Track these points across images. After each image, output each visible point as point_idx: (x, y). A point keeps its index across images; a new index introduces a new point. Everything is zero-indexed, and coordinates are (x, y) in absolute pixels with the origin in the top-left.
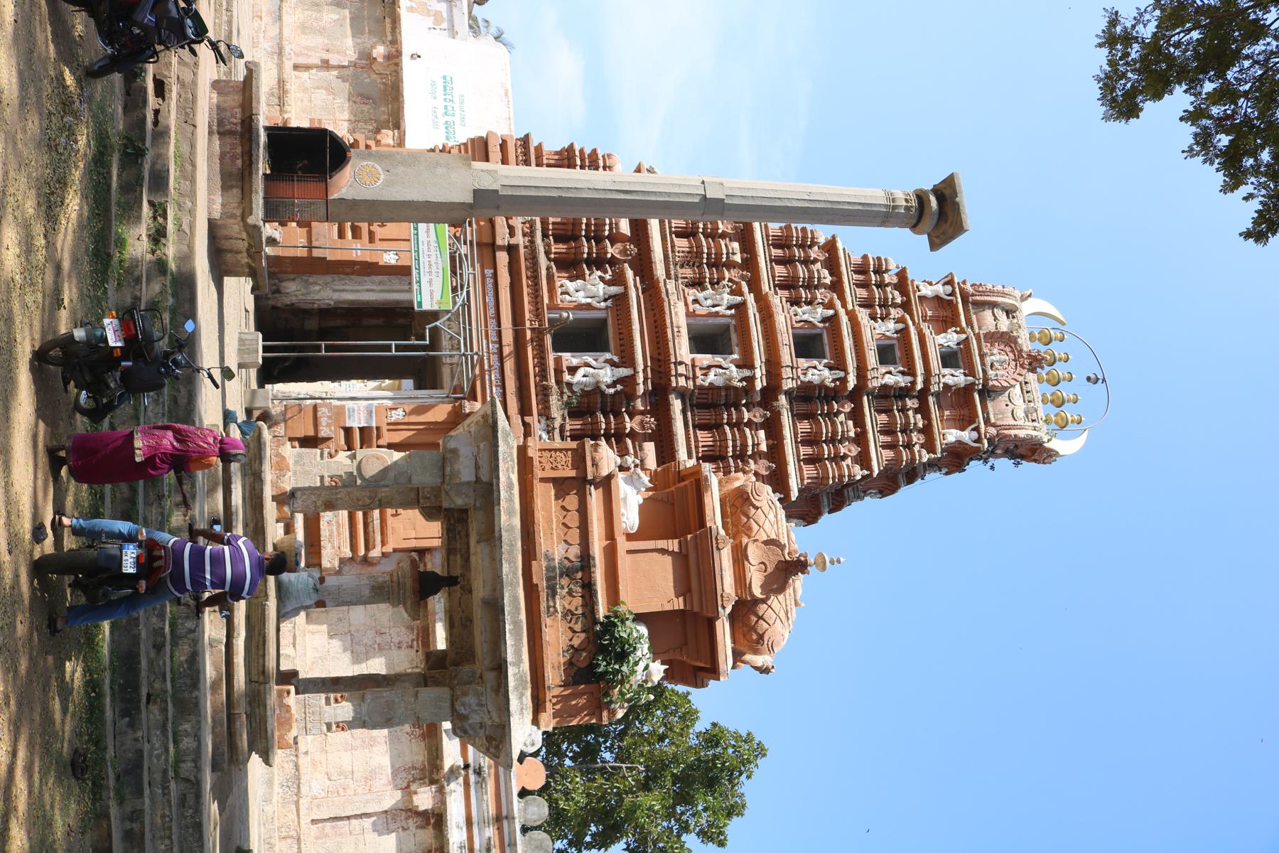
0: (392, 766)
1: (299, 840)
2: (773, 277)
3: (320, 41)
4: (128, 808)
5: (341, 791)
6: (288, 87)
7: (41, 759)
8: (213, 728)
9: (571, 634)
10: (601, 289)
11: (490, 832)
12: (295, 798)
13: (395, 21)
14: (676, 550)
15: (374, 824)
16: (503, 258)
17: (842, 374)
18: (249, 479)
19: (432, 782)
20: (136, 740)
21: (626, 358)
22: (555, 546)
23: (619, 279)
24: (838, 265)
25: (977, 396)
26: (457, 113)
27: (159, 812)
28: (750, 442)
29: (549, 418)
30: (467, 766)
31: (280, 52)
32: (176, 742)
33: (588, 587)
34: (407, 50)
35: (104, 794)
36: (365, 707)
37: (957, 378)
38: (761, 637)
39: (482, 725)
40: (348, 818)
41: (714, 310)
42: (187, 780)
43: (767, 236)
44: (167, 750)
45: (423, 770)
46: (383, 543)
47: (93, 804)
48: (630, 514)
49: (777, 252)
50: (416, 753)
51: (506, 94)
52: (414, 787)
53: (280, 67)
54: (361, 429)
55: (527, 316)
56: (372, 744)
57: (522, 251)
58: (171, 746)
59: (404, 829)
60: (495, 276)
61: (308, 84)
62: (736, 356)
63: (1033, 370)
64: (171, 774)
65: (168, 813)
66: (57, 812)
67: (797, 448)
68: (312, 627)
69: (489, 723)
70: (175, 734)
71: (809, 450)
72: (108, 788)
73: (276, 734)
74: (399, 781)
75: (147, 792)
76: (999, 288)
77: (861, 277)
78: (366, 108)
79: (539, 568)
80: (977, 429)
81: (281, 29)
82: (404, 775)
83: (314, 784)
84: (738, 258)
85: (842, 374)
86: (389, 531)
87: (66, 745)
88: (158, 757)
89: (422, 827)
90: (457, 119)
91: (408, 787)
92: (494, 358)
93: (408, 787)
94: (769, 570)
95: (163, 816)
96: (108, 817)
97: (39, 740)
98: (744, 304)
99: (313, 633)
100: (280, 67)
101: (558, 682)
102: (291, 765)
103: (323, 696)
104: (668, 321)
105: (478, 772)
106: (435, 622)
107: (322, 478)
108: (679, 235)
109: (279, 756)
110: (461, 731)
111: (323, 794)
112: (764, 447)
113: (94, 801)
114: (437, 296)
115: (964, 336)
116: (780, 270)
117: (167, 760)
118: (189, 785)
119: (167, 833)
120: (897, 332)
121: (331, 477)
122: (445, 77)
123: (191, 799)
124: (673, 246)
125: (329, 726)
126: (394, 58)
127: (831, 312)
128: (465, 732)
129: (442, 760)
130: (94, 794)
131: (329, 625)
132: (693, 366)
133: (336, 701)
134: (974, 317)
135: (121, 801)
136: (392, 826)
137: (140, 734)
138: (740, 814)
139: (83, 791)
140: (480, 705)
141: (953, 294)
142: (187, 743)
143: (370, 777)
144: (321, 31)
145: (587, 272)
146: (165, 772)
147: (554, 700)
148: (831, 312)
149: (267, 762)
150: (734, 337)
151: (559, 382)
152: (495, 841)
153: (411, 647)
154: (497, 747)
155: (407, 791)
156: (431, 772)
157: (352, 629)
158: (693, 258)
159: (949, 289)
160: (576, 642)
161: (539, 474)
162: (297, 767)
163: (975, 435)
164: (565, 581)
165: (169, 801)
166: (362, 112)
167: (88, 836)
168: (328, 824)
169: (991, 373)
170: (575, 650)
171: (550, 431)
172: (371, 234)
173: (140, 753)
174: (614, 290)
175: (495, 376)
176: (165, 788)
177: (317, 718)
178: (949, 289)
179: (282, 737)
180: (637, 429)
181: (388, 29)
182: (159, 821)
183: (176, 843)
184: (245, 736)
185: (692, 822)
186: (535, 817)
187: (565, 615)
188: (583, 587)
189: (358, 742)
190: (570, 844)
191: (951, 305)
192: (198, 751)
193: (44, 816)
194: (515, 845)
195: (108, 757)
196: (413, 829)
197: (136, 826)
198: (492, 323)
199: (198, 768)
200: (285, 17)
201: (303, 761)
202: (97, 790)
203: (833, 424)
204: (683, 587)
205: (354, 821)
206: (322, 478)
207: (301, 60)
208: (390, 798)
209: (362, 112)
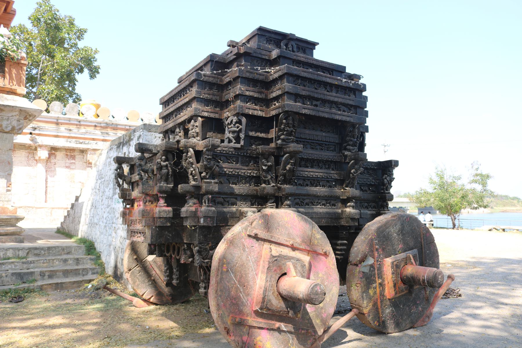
0: (26, 166)
1: (53, 208)
4: (39, 277)
7: (15, 316)
8: (2, 242)
11: (62, 128)
12: (34, 209)
15: (51, 176)
19: (36, 149)
20: (6, 276)
27: (42, 264)
30: (31, 133)
32: (9, 259)
35: (32, 288)
39: (18, 121)
40: (46, 187)
42: (28, 253)
44: (13, 263)
47: (36, 292)
52: (37, 158)
58: (10, 261)
59: (55, 164)
64: (24, 260)
65: (42, 261)
66: (40, 306)
69: (18, 117)
70: (5, 259)
72: (29, 287)
73: (9, 214)
74: (33, 164)
75: (32, 270)
82: (30, 162)
87: (7, 306)
88: (15, 266)
89: (55, 157)
91: (36, 160)
93: (36, 160)
95: (44, 263)
96: (42, 286)
97: (6, 318)
105: (35, 129)
109: (20, 213)
110: (19, 131)
113: (34, 292)
117: (18, 262)
118: (30, 252)
119: (51, 261)
123: (36, 252)
125: (8, 191)
128: (20, 129)
129: (26, 144)
130: (31, 292)
135: (36, 281)
136: (53, 169)
137: (4, 275)
138: (74, 20)
139: (30, 297)
140: (8, 119)
142: (10, 254)
146: (23, 263)
147: (11, 84)
149: (22, 219)
152: (67, 127)
154: (30, 116)
156: (31, 149)
165: (37, 261)
167: (49, 293)
168: (48, 196)
173: (13, 274)
176: (31, 262)
179: (11, 212)
182: (45, 265)
183: (56, 257)
184: (8, 228)
185: (73, 41)
186: (59, 108)
190: (71, 96)
192: (14, 249)
193: (42, 311)
194: (70, 119)
195: (14, 288)
196: (55, 161)
197: (47, 274)
199: (23, 249)
202: (29, 291)
205: (48, 185)
208: (40, 168)
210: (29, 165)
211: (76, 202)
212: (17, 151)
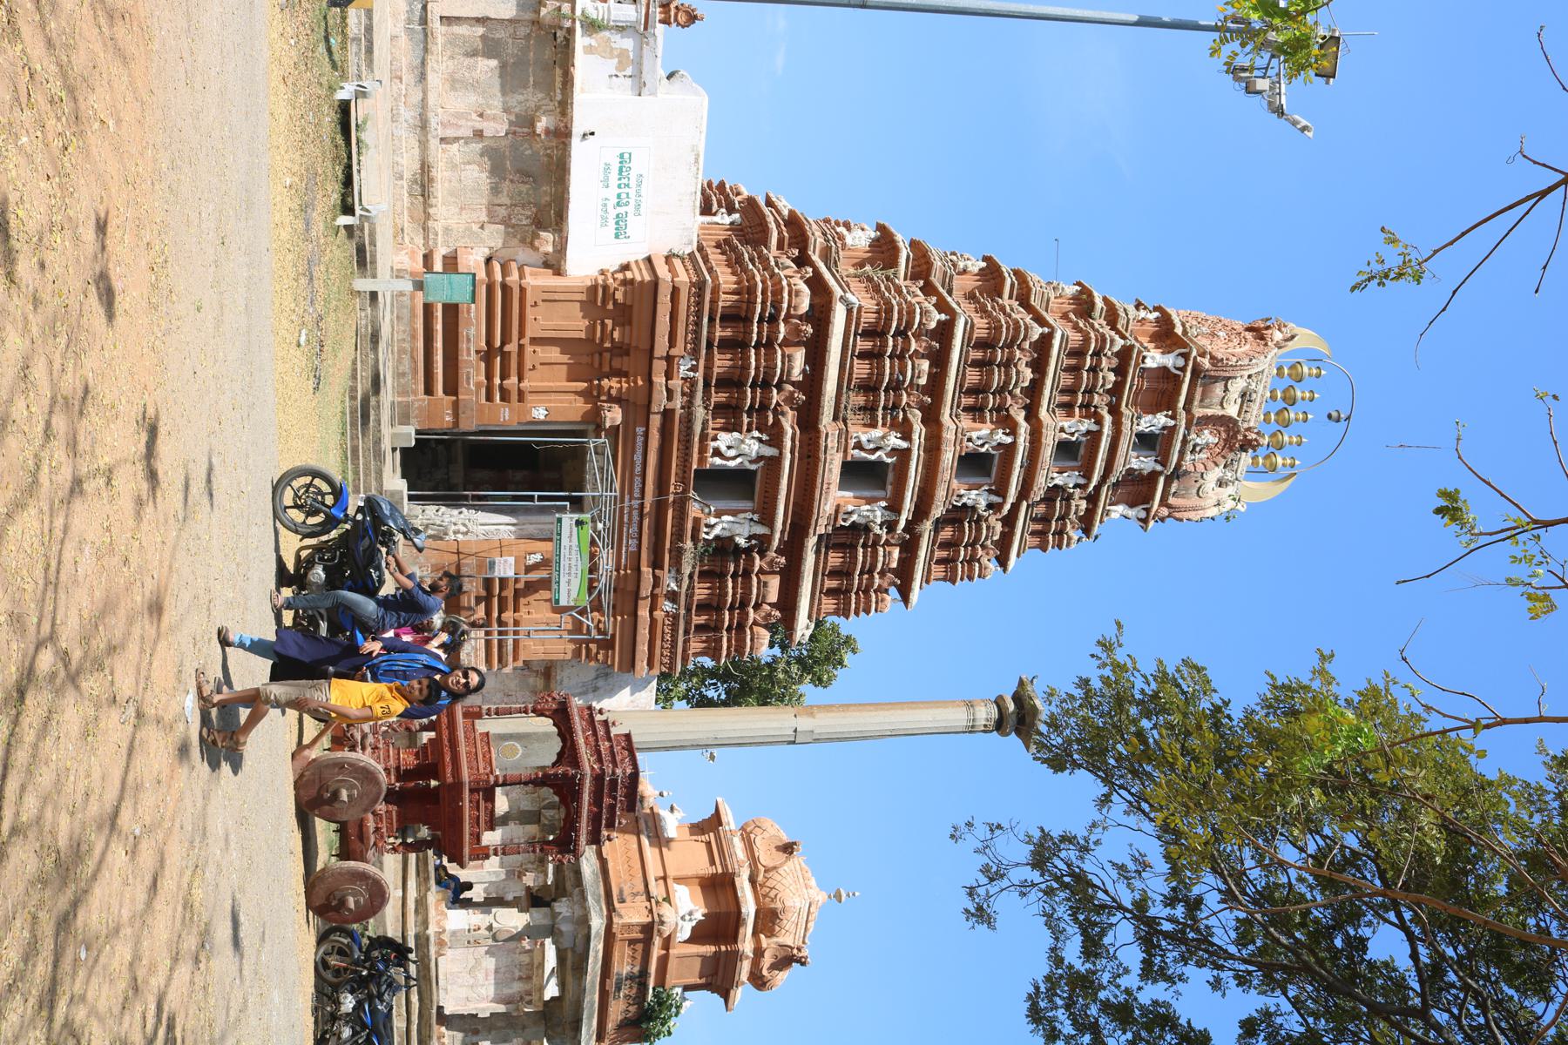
2: (961, 386)
3: (472, 98)
6: (434, 173)
10: (752, 446)
13: (568, 81)
16: (656, 421)
17: (999, 500)
21: (767, 518)
23: (775, 439)
24: (1046, 363)
25: (1162, 480)
26: (632, 202)
28: (879, 566)
29: (679, 571)
31: (424, 125)
33: (643, 986)
34: (577, 129)
37: (1144, 463)
38: (764, 984)
41: (873, 457)
43: (970, 339)
46: (515, 659)
49: (976, 355)
51: (697, 161)
53: (423, 145)
54: (501, 580)
55: (673, 480)
57: (679, 412)
60: (646, 435)
61: (458, 160)
62: (884, 504)
63: (1243, 448)
67: (932, 552)
71: (944, 554)
76: (1246, 362)
77: (1073, 362)
78: (524, 188)
79: (611, 985)
80: (1148, 511)
81: (425, 92)
84: (923, 381)
85: (999, 500)
90: (630, 209)
92: (635, 513)
98: (909, 450)
100: (423, 145)
104: (819, 480)
108: (863, 355)
112: (894, 565)
114: (574, 595)
115: (1172, 423)
116: (973, 376)
120: (1088, 432)
122: (622, 156)
124: (851, 374)
126: (562, 135)
127: (1009, 440)
132: (837, 511)
134: (1199, 390)
141: (1183, 369)
144: (474, 86)
145: (746, 420)
148: (1009, 440)
150: (890, 477)
151: (695, 538)
158: (869, 387)
159: (1181, 362)
161: (619, 936)
163: (1143, 515)
166: (520, 193)
169: (1188, 457)
171: (679, 582)
172: (521, 394)
174: (769, 451)
175: (635, 528)
178: (1181, 362)
180: (765, 567)
181: (558, 85)
191: (1178, 381)
198: (638, 480)
200: (431, 76)
203: (979, 530)
207: (450, 133)
209: (520, 193)
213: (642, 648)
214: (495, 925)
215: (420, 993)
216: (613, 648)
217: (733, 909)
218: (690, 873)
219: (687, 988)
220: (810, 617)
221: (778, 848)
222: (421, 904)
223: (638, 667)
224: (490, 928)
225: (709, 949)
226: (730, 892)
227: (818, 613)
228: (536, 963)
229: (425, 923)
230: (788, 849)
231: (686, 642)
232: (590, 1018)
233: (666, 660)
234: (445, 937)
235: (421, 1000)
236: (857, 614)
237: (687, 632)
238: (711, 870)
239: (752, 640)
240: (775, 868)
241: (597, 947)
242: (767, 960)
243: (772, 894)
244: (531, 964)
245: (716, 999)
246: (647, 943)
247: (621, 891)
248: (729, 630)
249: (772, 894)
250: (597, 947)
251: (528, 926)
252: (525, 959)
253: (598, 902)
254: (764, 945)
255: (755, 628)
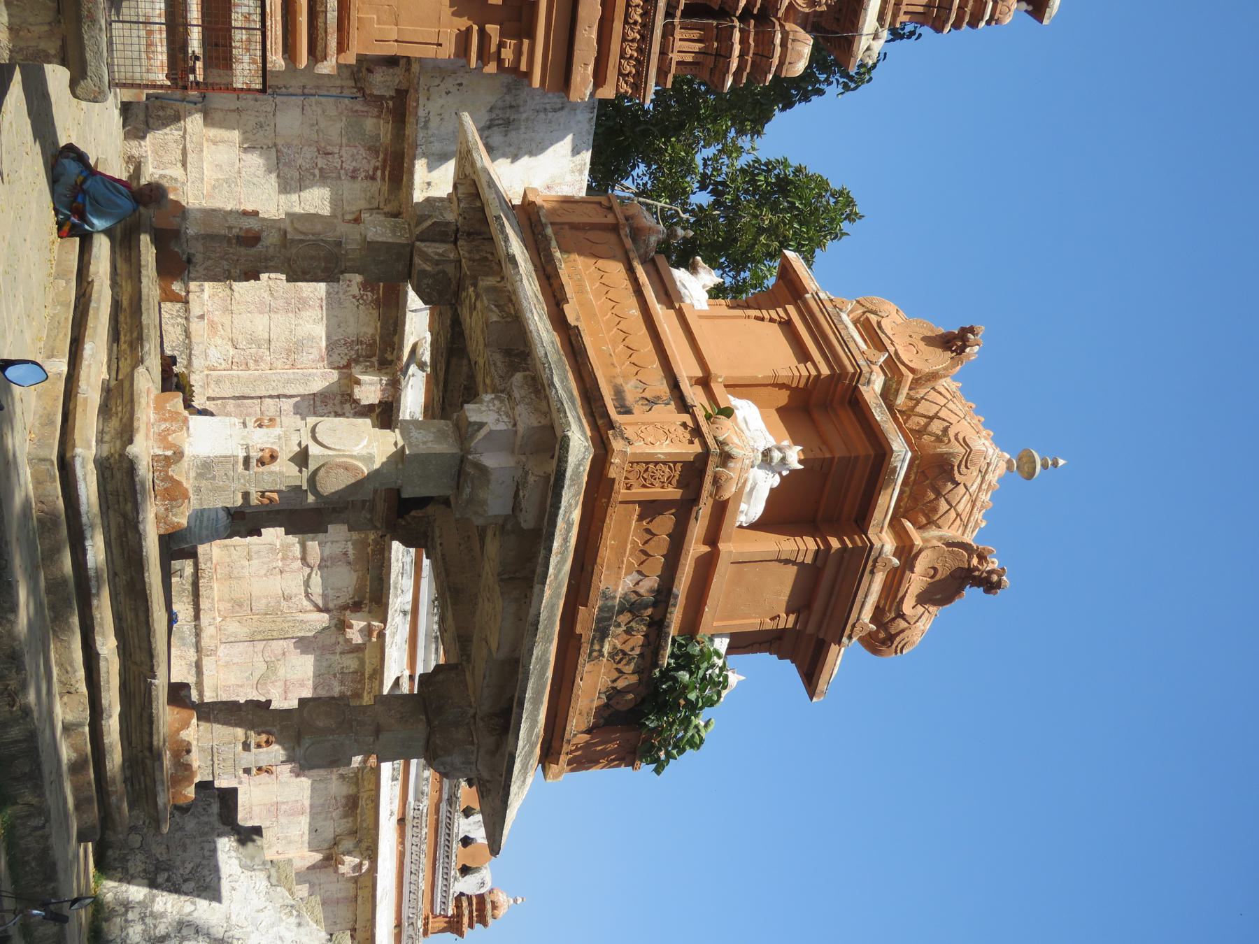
0: (328, 338)
5: (251, 363)
9: (616, 675)
14: (809, 560)
15: (296, 406)
18: (114, 520)
22: (619, 580)
33: (657, 626)
36: (300, 752)
38: (891, 638)
45: (371, 345)
46: (341, 48)
48: (752, 509)
50: (365, 324)
56: (301, 305)
68: (213, 132)
74: (336, 357)
82: (344, 350)
83: (212, 352)
86: (354, 23)
91: (348, 366)
93: (348, 366)
94: (938, 577)
99: (215, 143)
101: (584, 727)
102: (179, 330)
103: (240, 732)
106: (414, 158)
107: (246, 495)
111: (224, 365)
121: (263, 494)
131: (245, 133)
133: (259, 746)
143: (294, 350)
153: (373, 178)
155: (345, 368)
156: (383, 351)
157: (280, 141)
160: (621, 684)
161: (621, 492)
162: (187, 334)
164: (624, 618)
170: (613, 694)
177: (230, 763)
187: (612, 656)
188: (650, 625)
189: (281, 302)
201: (195, 326)
204: (801, 602)
206: (246, 495)
208: (322, 378)
210: (331, 346)
211: (215, 808)
212: (375, 313)
213: (587, 35)
214: (314, 450)
215: (120, 633)
216: (532, 36)
217: (862, 448)
218: (761, 372)
219: (742, 643)
220: (881, 18)
221: (929, 341)
222: (118, 398)
223: (576, 78)
224: (302, 458)
225: (806, 546)
226: (848, 419)
227: (895, 16)
228: (368, 670)
229: (127, 433)
230: (954, 342)
231: (668, 31)
232: (537, 702)
233: (629, 68)
234: (184, 474)
235: (124, 650)
236: (957, 25)
237: (669, 14)
238: (806, 370)
239: (784, 44)
240: (934, 376)
241: (571, 511)
242: (916, 582)
243: (936, 427)
244: (359, 673)
245: (787, 671)
246: (684, 509)
247: (619, 394)
248: (745, 16)
249: (936, 427)
250: (571, 511)
251: (399, 457)
252: (351, 663)
253: (573, 403)
254: (918, 542)
255: (788, 26)
